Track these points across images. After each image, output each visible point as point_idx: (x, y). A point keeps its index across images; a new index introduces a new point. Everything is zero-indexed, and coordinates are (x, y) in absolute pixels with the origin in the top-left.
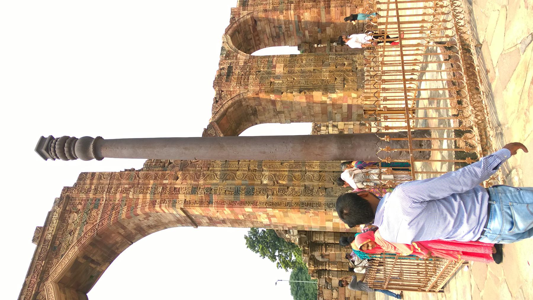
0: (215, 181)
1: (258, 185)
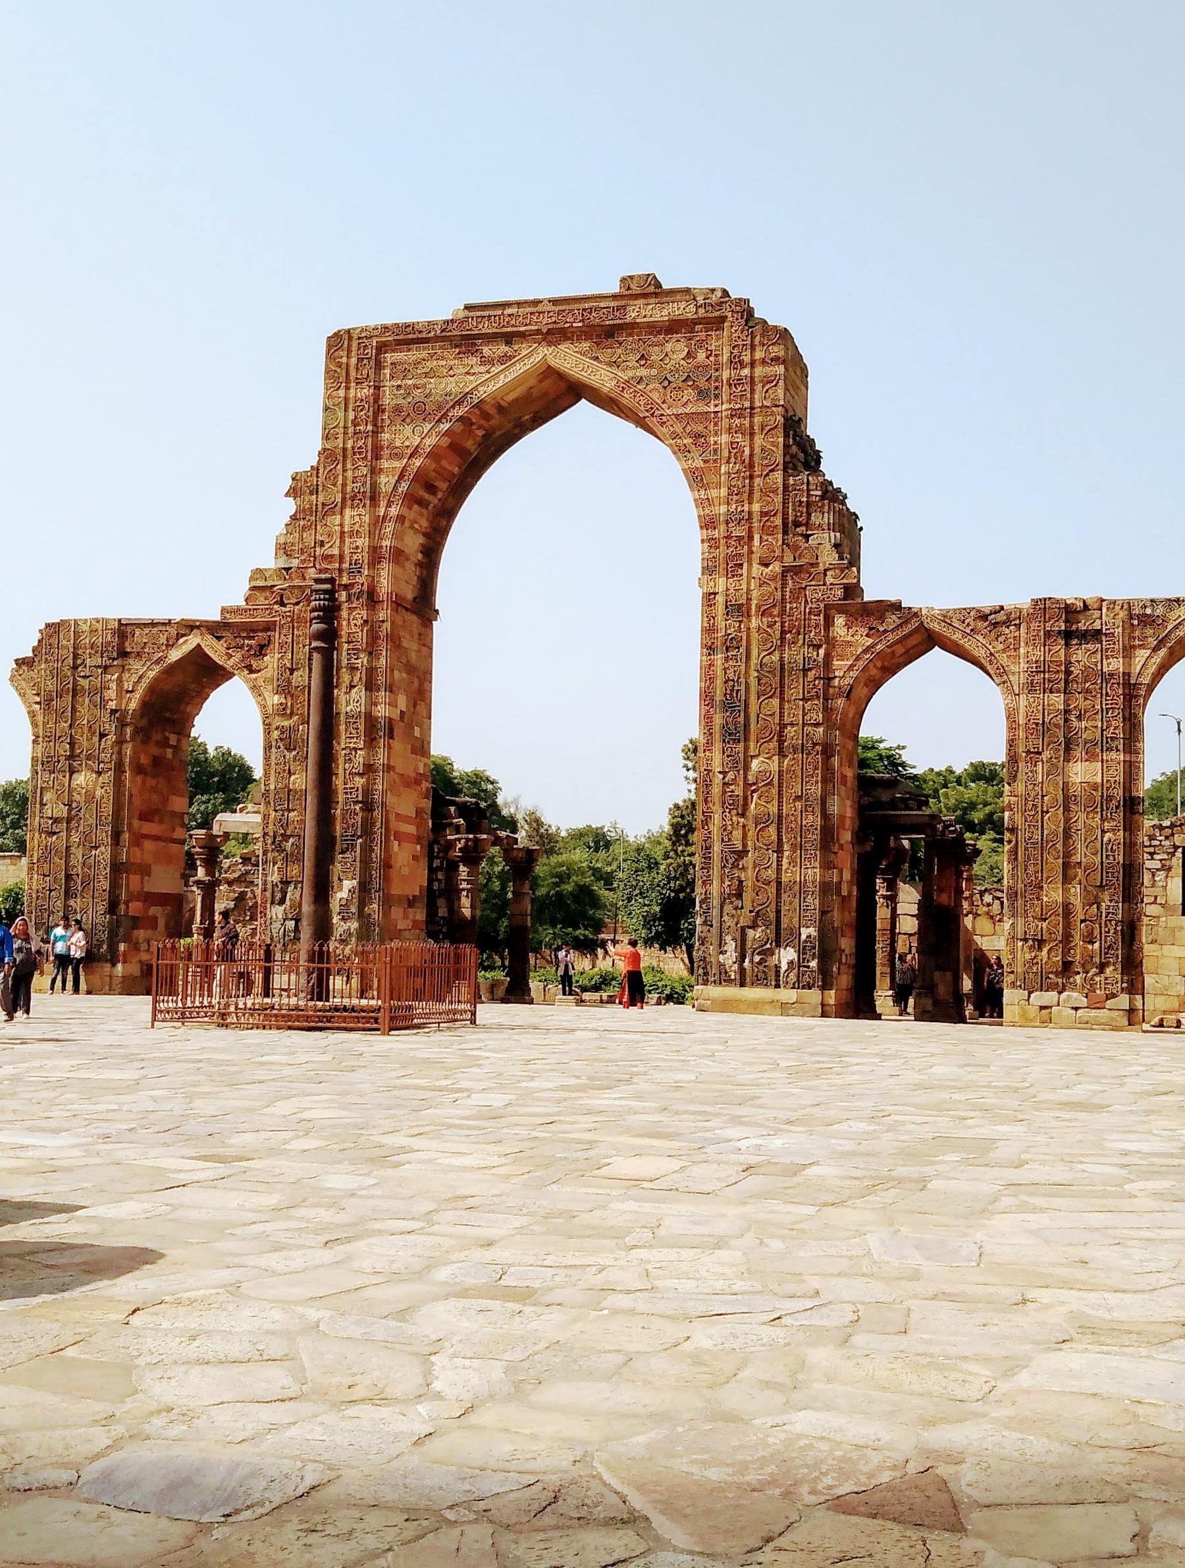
0: (754, 652)
1: (746, 749)
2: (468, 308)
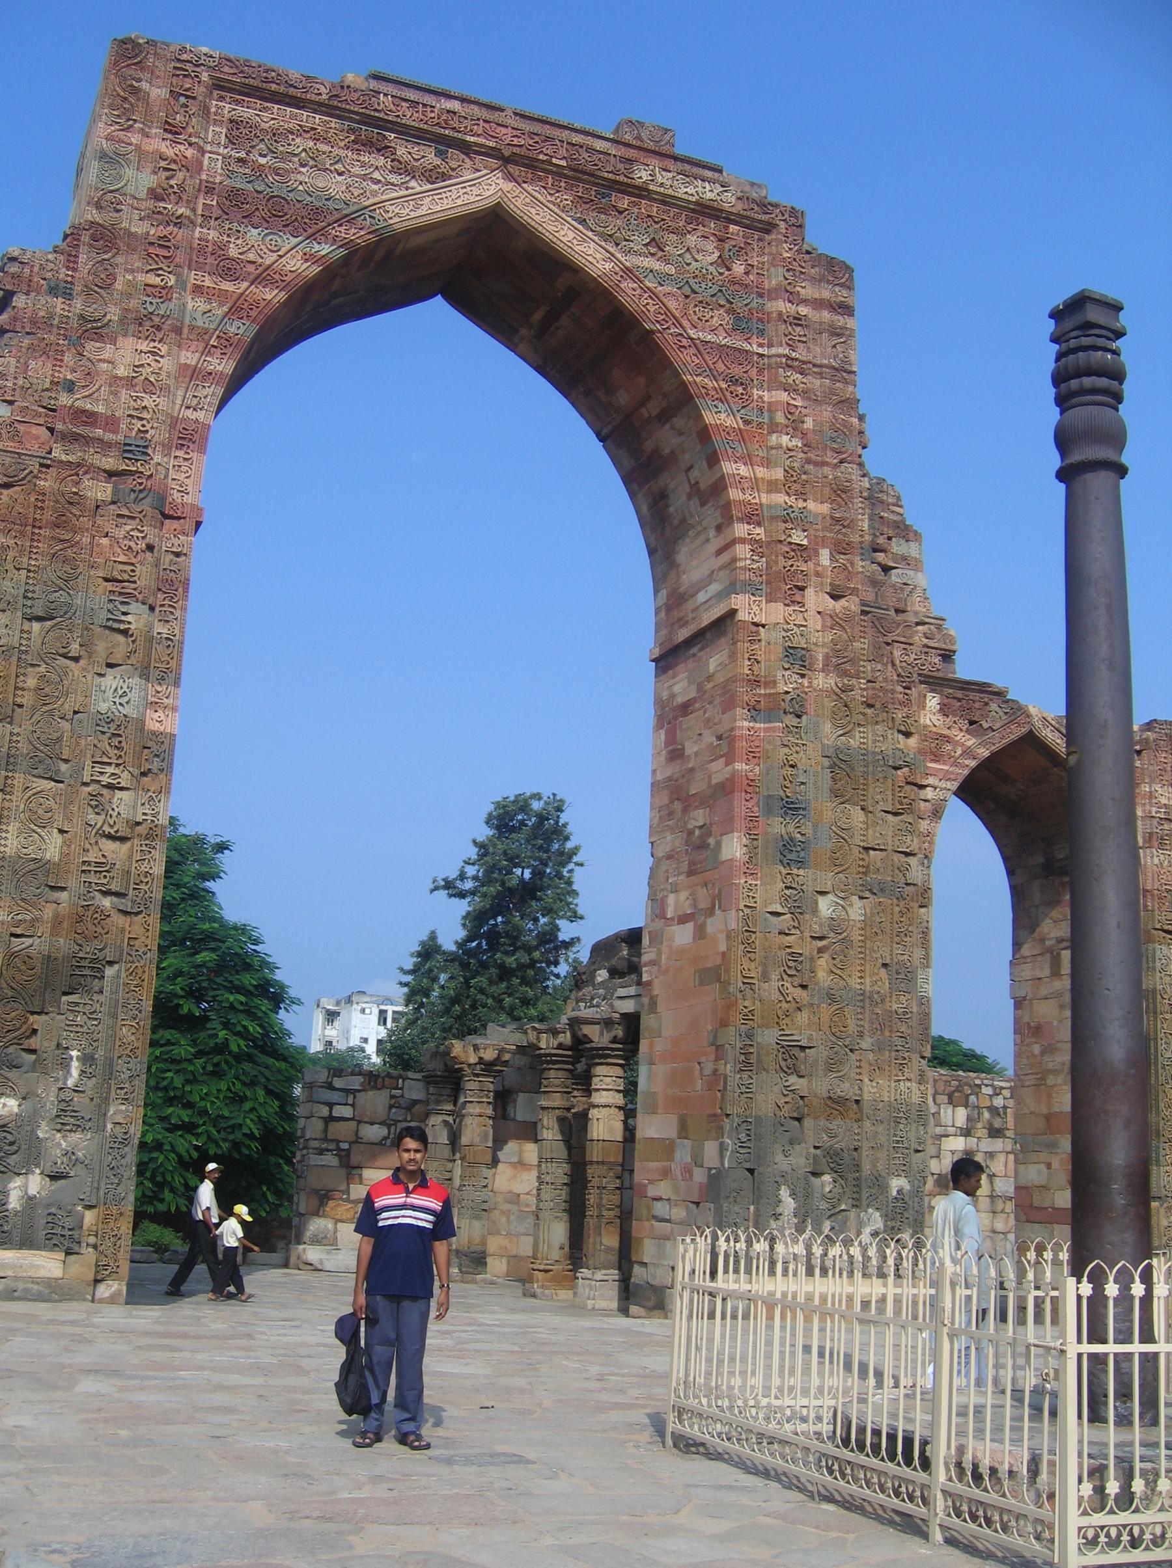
2: (376, 77)
